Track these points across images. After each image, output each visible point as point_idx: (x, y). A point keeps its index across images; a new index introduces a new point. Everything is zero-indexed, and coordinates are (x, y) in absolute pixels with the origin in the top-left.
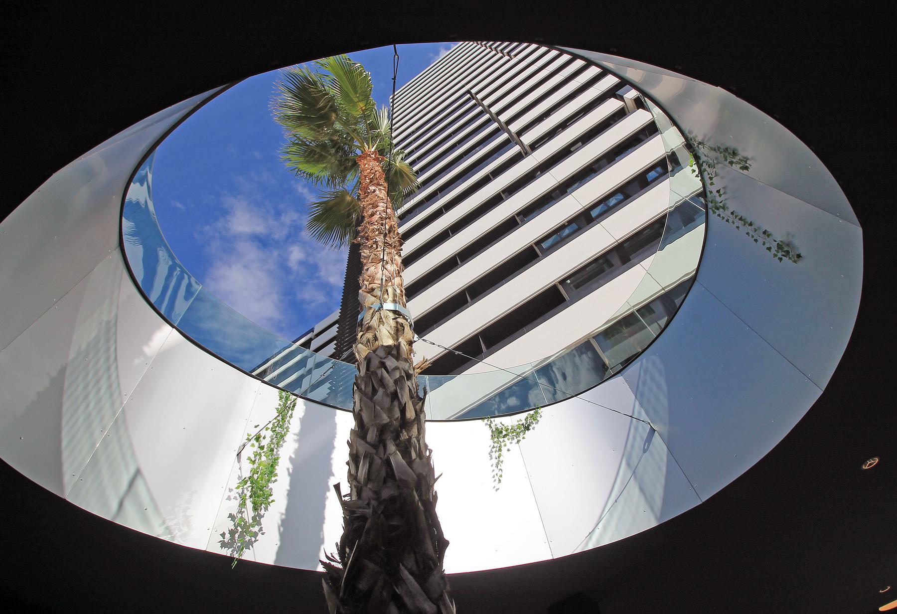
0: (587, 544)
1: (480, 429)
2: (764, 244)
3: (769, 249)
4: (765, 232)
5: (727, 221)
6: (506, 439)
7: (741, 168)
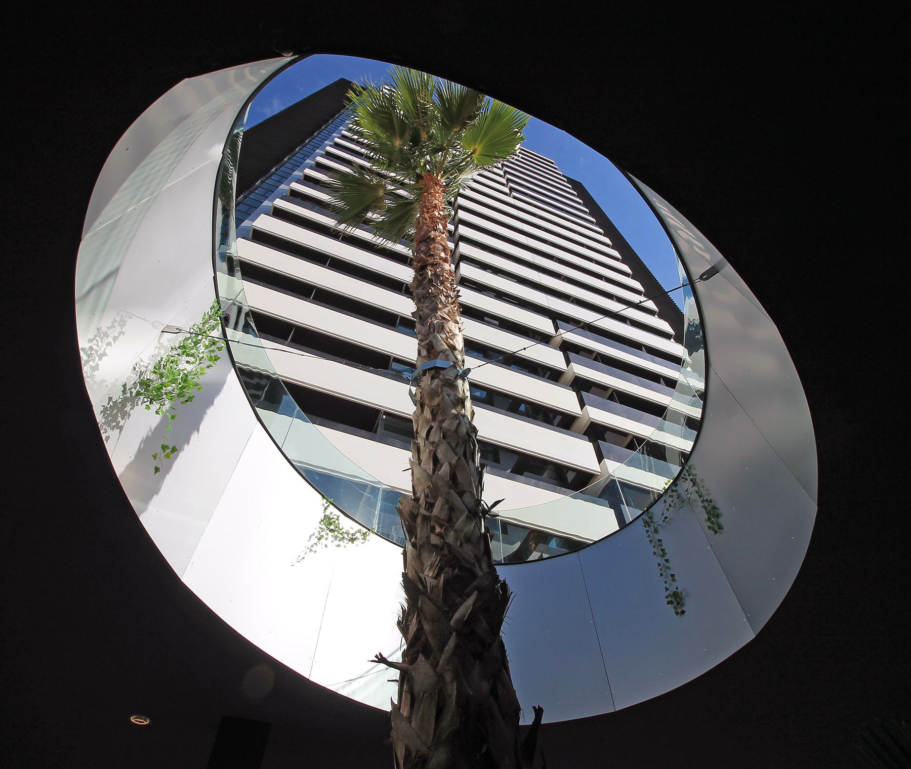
0: (344, 687)
1: (313, 504)
2: (666, 582)
3: (667, 589)
4: (673, 576)
5: (651, 541)
6: (330, 534)
7: (709, 527)
